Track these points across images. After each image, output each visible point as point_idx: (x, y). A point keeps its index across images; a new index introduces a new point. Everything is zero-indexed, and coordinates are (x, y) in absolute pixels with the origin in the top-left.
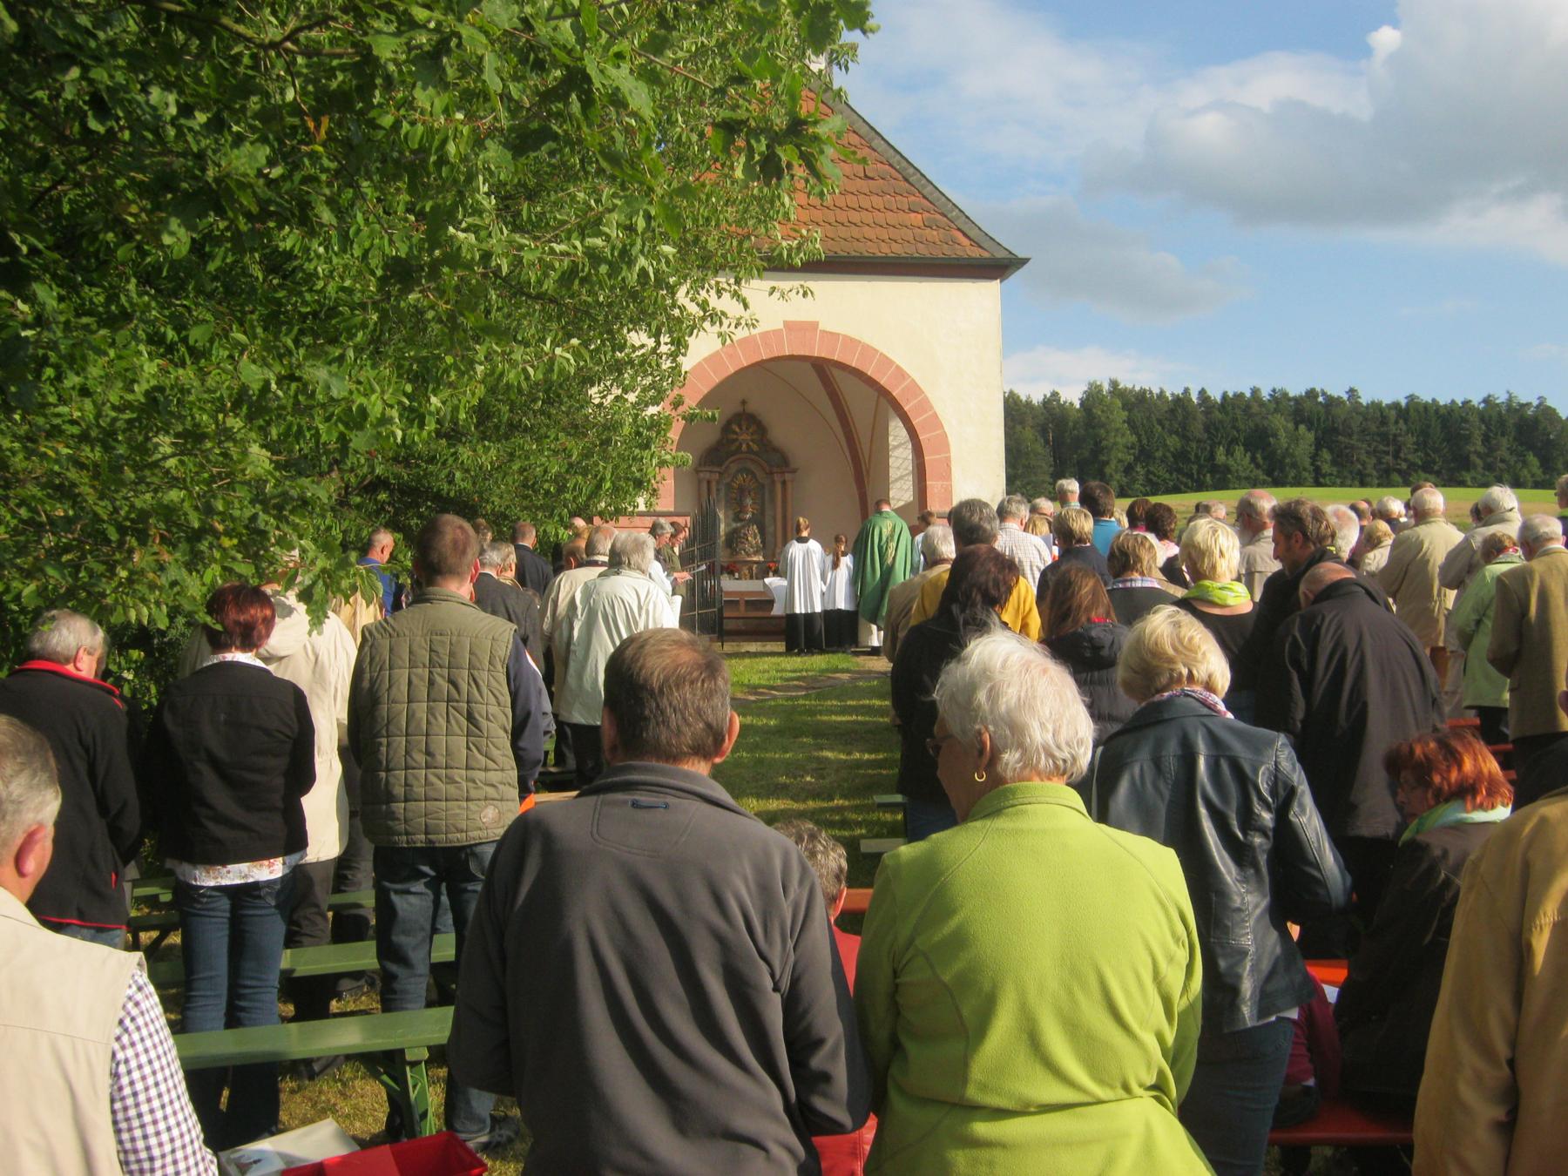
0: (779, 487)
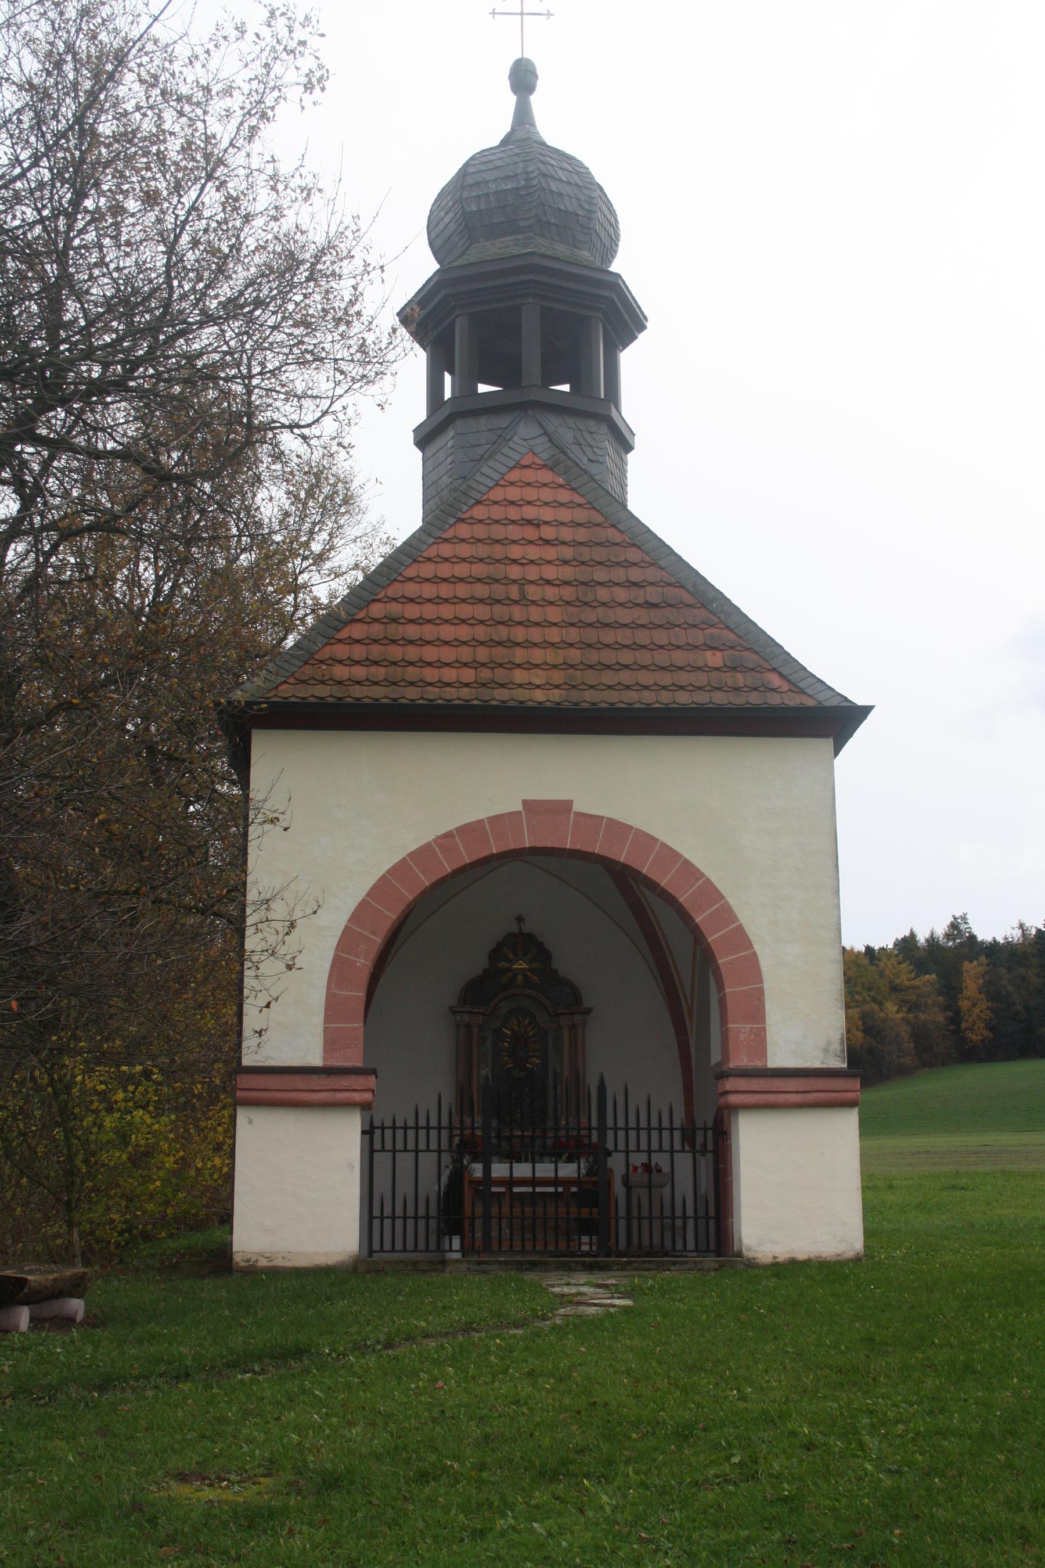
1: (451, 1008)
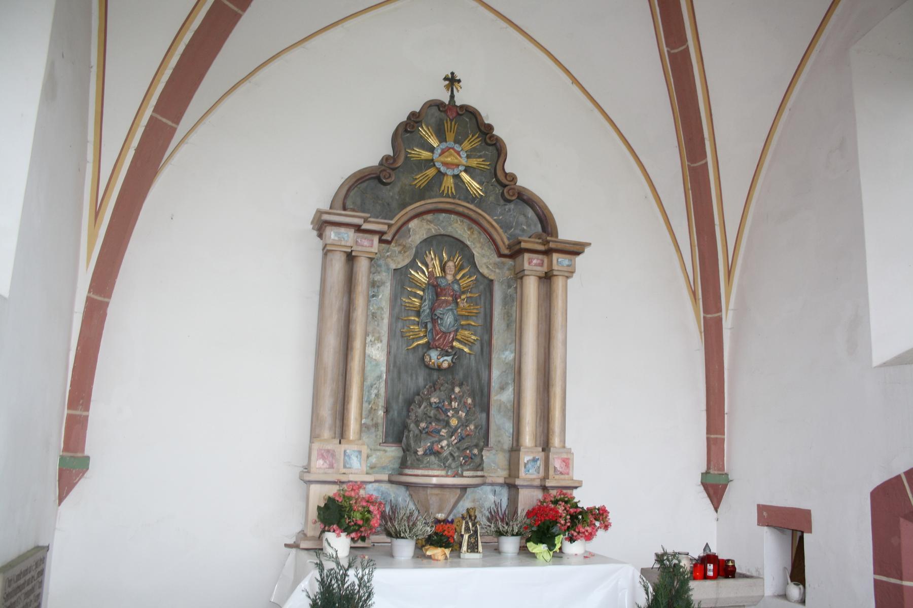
0: (531, 287)
1: (320, 213)
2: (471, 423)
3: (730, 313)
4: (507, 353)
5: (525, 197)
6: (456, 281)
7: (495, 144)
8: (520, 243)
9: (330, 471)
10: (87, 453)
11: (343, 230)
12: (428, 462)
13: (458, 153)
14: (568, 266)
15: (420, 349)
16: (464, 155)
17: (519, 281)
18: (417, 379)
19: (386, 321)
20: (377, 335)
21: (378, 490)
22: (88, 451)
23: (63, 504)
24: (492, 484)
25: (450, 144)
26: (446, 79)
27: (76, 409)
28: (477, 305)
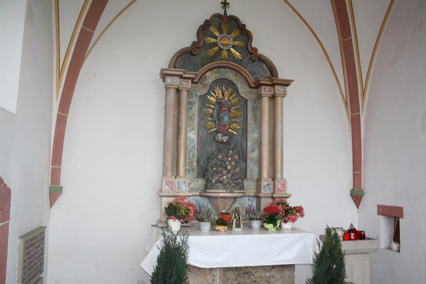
0: (266, 102)
1: (163, 70)
2: (237, 167)
3: (364, 113)
4: (255, 134)
5: (262, 59)
6: (229, 100)
7: (246, 34)
8: (259, 81)
9: (171, 191)
10: (61, 185)
11: (174, 78)
12: (217, 186)
13: (229, 39)
14: (283, 91)
15: (213, 133)
16: (232, 40)
17: (260, 99)
18: (212, 147)
19: (196, 120)
20: (192, 127)
21: (194, 200)
22: (61, 185)
23: (52, 208)
24: (249, 196)
25: (225, 34)
26: (222, 3)
27: (55, 165)
28: (240, 111)
